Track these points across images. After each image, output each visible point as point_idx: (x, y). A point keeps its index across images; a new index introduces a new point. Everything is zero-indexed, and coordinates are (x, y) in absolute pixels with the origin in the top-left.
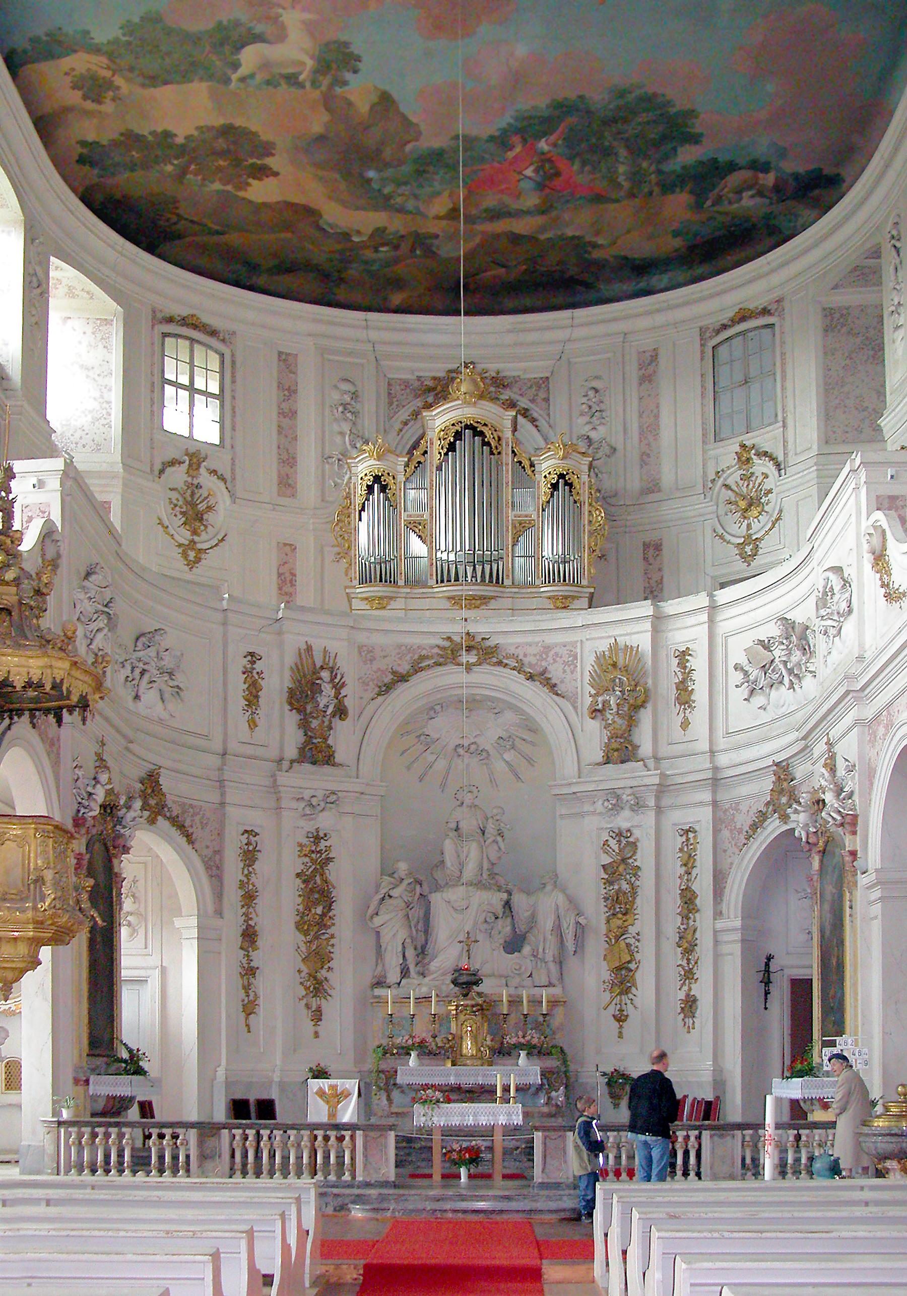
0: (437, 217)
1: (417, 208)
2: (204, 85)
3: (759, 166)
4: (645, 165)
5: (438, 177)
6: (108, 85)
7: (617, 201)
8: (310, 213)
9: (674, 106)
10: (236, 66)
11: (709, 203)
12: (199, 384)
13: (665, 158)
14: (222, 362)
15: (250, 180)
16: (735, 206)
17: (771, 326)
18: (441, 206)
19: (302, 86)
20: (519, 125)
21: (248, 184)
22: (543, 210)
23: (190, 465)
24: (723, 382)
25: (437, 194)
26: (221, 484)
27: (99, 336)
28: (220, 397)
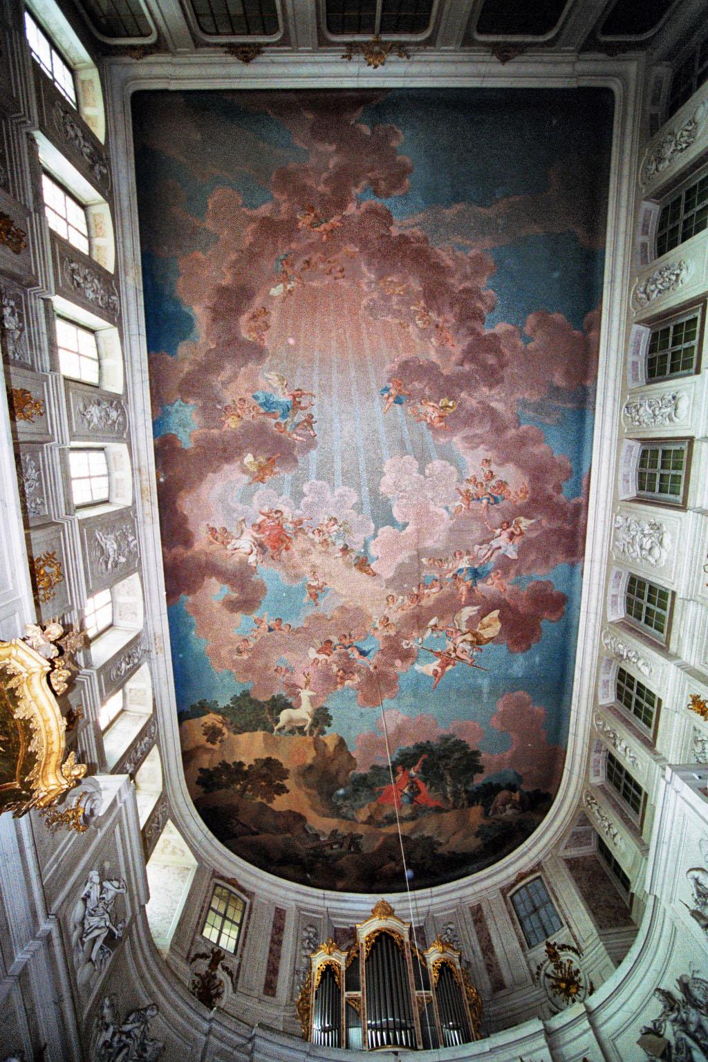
0: (364, 823)
1: (353, 815)
2: (262, 732)
3: (512, 788)
4: (459, 786)
5: (363, 794)
6: (220, 733)
7: (448, 811)
8: (300, 818)
9: (469, 748)
10: (277, 721)
11: (491, 812)
12: (229, 915)
13: (467, 783)
14: (245, 907)
15: (276, 796)
16: (504, 814)
17: (539, 878)
18: (363, 815)
19: (304, 734)
20: (401, 758)
21: (274, 799)
22: (413, 818)
23: (212, 961)
24: (523, 914)
25: (362, 806)
26: (229, 979)
27: (181, 875)
28: (240, 925)
